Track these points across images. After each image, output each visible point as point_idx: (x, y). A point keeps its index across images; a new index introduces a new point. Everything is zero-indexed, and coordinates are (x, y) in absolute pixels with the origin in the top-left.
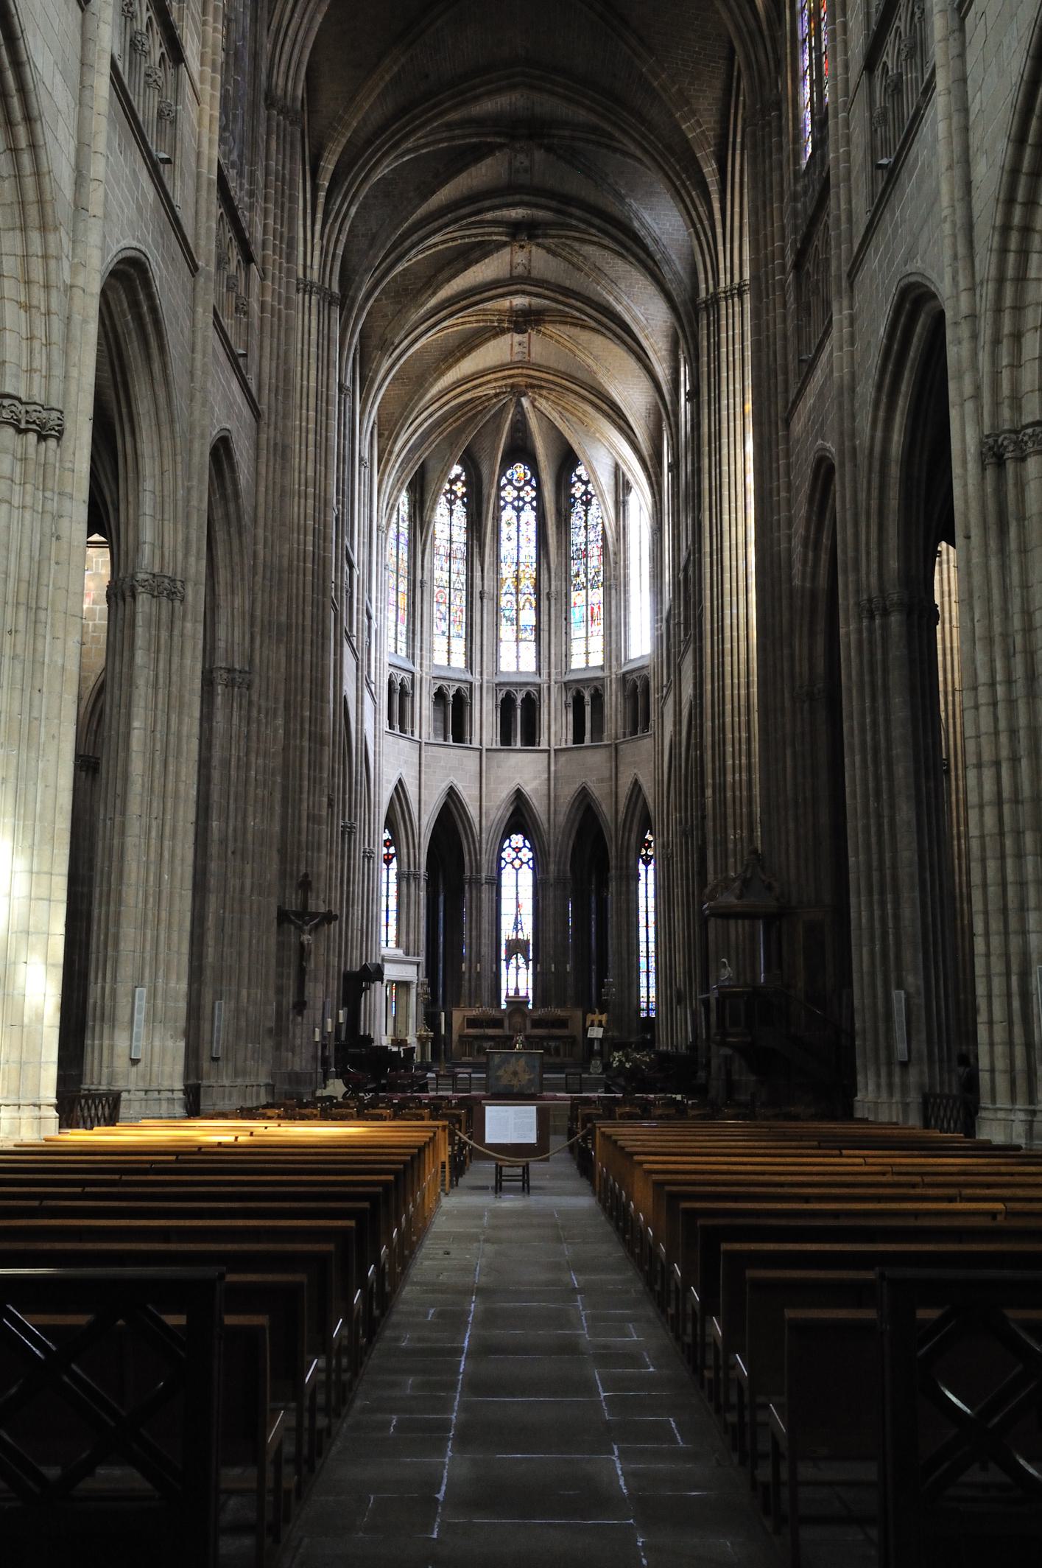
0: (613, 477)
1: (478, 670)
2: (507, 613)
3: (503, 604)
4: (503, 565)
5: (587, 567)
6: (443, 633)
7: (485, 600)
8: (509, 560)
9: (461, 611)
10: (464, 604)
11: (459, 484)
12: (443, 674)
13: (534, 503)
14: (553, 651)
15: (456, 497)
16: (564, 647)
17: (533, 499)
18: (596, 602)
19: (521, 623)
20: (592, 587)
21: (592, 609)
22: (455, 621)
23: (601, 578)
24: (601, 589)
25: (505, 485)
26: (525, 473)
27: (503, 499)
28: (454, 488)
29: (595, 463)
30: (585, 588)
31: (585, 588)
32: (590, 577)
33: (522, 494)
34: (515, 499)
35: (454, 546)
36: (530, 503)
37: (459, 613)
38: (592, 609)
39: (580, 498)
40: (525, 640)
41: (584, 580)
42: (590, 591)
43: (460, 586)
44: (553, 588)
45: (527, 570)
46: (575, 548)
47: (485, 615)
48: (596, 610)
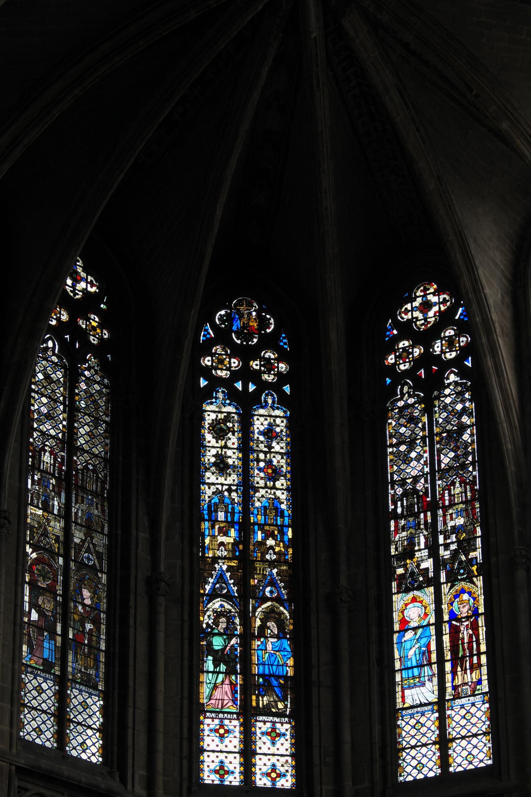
0: (507, 300)
1: (141, 772)
2: (218, 643)
3: (206, 620)
4: (205, 525)
5: (434, 534)
6: (47, 667)
7: (161, 600)
8: (221, 516)
9: (96, 622)
10: (104, 606)
11: (95, 320)
12: (44, 764)
13: (287, 389)
14: (347, 737)
15: (87, 346)
16: (377, 728)
17: (282, 378)
18: (464, 611)
19: (255, 670)
20: (452, 579)
21: (455, 632)
22: (78, 643)
23: (477, 554)
24: (479, 582)
25: (210, 343)
26: (263, 323)
27: (207, 372)
28: (82, 324)
29: (472, 246)
30: (436, 583)
31: (436, 583)
32: (444, 554)
33: (255, 365)
34: (235, 376)
35: (80, 460)
36: (276, 387)
37: (89, 626)
38: (455, 632)
39: (410, 373)
40: (267, 711)
41: (428, 564)
42: (445, 589)
43: (93, 561)
44: (343, 581)
45: (270, 542)
46: (400, 491)
47: (161, 636)
48: (465, 634)
